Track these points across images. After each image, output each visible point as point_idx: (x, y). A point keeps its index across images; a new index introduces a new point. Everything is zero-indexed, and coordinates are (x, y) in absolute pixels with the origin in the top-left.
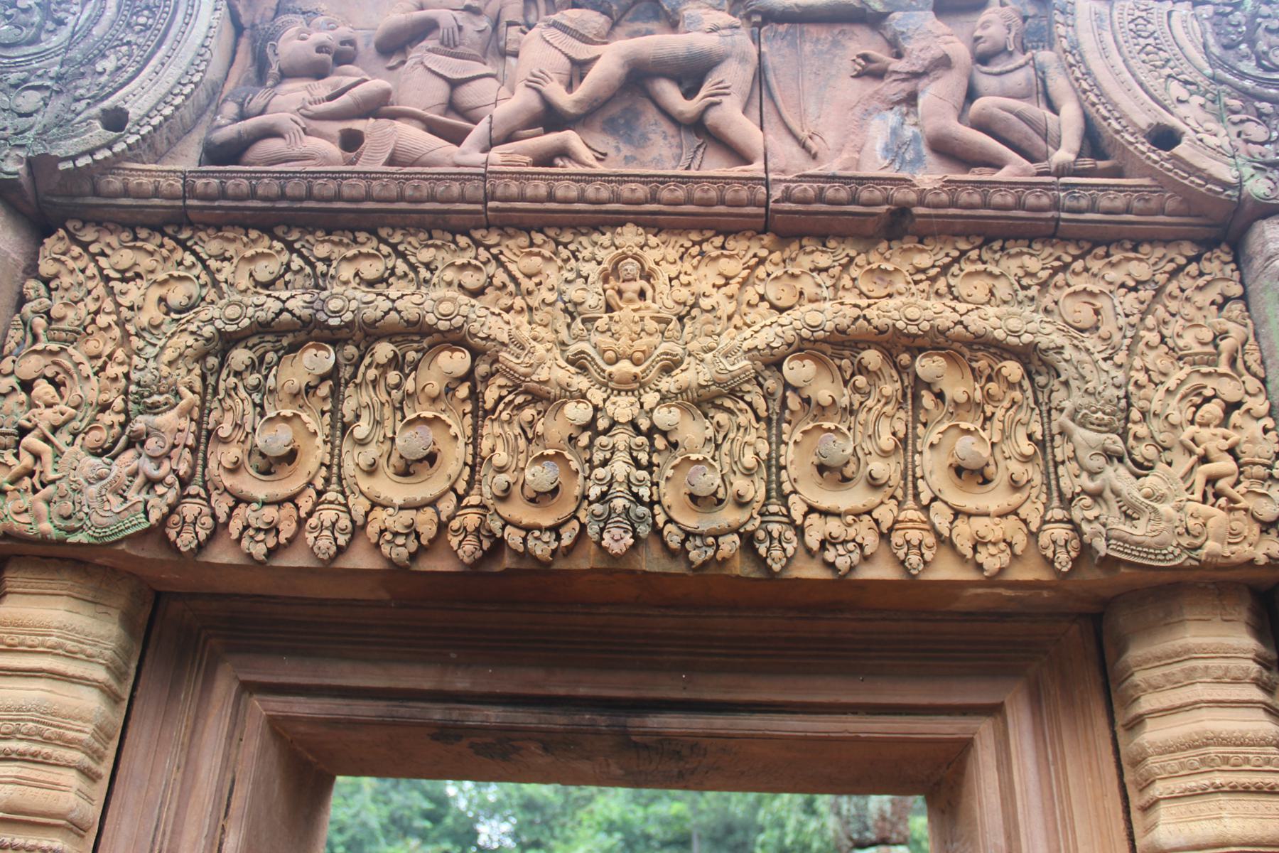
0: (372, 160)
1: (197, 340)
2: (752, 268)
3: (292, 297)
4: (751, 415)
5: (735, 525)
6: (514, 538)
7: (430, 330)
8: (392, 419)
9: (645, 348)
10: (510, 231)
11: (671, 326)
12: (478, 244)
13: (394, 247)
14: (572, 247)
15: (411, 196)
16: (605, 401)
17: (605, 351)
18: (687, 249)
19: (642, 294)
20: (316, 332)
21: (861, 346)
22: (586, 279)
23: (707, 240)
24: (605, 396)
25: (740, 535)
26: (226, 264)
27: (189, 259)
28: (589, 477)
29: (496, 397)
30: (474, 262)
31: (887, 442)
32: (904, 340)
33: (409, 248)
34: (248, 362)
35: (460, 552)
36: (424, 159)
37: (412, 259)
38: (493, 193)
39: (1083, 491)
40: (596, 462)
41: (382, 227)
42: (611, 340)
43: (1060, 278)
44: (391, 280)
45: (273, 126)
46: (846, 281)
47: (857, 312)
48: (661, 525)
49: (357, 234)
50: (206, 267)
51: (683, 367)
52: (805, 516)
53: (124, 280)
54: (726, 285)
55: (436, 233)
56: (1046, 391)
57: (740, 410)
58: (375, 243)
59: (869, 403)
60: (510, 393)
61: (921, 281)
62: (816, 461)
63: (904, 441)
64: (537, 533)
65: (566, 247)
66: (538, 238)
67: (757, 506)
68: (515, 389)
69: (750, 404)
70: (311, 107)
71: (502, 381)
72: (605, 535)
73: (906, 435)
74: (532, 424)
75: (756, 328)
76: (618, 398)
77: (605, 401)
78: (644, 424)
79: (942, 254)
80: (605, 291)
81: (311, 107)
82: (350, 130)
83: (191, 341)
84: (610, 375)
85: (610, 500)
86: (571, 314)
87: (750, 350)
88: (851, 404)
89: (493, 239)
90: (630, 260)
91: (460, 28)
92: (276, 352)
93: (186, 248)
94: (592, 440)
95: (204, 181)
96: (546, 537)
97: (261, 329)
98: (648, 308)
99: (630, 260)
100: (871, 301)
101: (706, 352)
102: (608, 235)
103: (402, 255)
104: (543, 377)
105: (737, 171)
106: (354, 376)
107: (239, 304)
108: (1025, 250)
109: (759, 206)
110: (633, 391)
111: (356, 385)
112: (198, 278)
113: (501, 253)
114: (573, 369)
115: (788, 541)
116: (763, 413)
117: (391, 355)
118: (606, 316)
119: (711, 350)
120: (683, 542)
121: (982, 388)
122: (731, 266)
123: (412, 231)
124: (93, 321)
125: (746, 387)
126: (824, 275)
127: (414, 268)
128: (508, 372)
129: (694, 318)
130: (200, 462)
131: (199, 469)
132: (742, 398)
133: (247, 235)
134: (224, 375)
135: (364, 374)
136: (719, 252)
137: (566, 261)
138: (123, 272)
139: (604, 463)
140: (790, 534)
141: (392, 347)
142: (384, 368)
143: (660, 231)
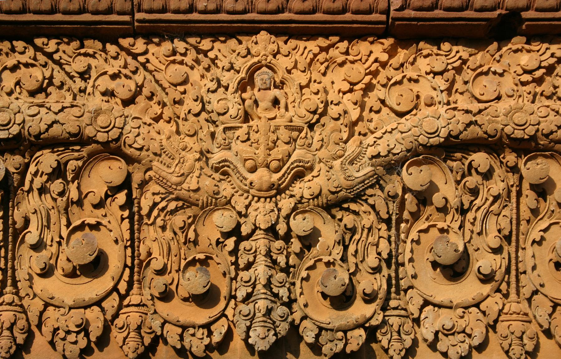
2: (375, 74)
5: (361, 321)
6: (172, 334)
7: (91, 140)
9: (280, 157)
11: (303, 135)
13: (50, 55)
14: (211, 55)
16: (247, 207)
17: (246, 160)
18: (315, 55)
22: (227, 88)
23: (332, 46)
24: (247, 202)
25: (366, 329)
28: (235, 278)
29: (151, 204)
30: (124, 71)
31: (493, 240)
33: (65, 57)
40: (242, 266)
42: (249, 149)
46: (459, 86)
51: (315, 173)
52: (421, 310)
54: (351, 91)
58: (31, 52)
62: (432, 259)
63: (508, 238)
64: (191, 331)
65: (206, 56)
66: (180, 46)
69: (373, 207)
72: (251, 333)
73: (511, 232)
74: (184, 229)
75: (378, 134)
76: (260, 204)
77: (247, 207)
78: (282, 228)
80: (244, 101)
84: (251, 183)
85: (255, 302)
86: (214, 122)
87: (373, 157)
88: (462, 204)
89: (140, 45)
90: (264, 69)
94: (237, 244)
96: (200, 333)
98: (282, 116)
99: (264, 69)
101: (334, 159)
104: (194, 186)
109: (381, 13)
110: (271, 197)
113: (148, 61)
114: (217, 176)
117: (55, 165)
118: (245, 126)
119: (340, 157)
120: (318, 336)
122: (357, 71)
123: (66, 40)
126: (438, 77)
128: (161, 181)
129: (323, 126)
135: (32, 182)
137: (208, 69)
141: (54, 156)
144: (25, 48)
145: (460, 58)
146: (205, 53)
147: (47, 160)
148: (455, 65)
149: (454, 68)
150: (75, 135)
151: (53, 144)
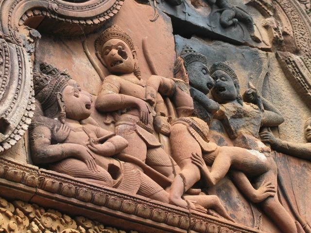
15: (156, 218)
36: (156, 195)
38: (194, 225)
45: (79, 152)
70: (95, 146)
81: (95, 146)
91: (150, 113)
95: (51, 180)
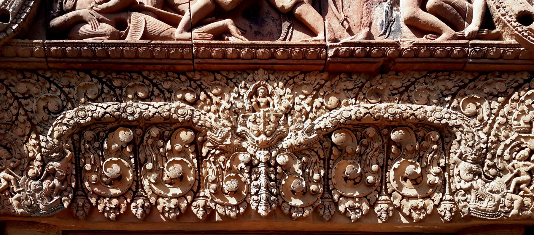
0: (134, 36)
1: (67, 127)
3: (108, 106)
4: (317, 157)
8: (161, 161)
10: (205, 73)
12: (191, 79)
13: (151, 81)
14: (234, 80)
18: (287, 81)
19: (268, 104)
20: (122, 123)
21: (366, 126)
23: (296, 76)
26: (71, 89)
27: (54, 88)
32: (386, 123)
34: (93, 136)
35: (197, 215)
37: (160, 87)
39: (461, 189)
41: (144, 70)
43: (462, 91)
44: (152, 97)
47: (366, 110)
48: (281, 203)
49: (132, 74)
50: (62, 92)
53: (25, 98)
55: (170, 74)
56: (449, 145)
57: (312, 155)
59: (368, 151)
60: (213, 149)
61: (396, 94)
65: (232, 81)
66: (218, 76)
67: (320, 195)
68: (215, 147)
71: (209, 144)
79: (406, 80)
82: (120, 18)
83: (65, 128)
92: (105, 131)
93: (51, 82)
97: (96, 122)
100: (373, 105)
102: (251, 75)
103: (155, 85)
105: (311, 40)
106: (142, 142)
107: (84, 109)
108: (447, 77)
111: (143, 146)
112: (60, 96)
115: (332, 209)
116: (322, 157)
121: (419, 143)
124: (17, 119)
125: (315, 146)
127: (162, 91)
130: (79, 181)
131: (80, 184)
132: (313, 150)
133: (78, 75)
134: (82, 142)
135: (147, 141)
136: (302, 82)
138: (23, 94)
139: (256, 179)
140: (332, 206)
141: (158, 129)
142: (156, 139)
143: (275, 71)
144: (138, 77)
145: (361, 82)
146: (231, 80)
147: (155, 132)
148: (359, 85)
149: (358, 87)
150: (168, 119)
151: (156, 125)
